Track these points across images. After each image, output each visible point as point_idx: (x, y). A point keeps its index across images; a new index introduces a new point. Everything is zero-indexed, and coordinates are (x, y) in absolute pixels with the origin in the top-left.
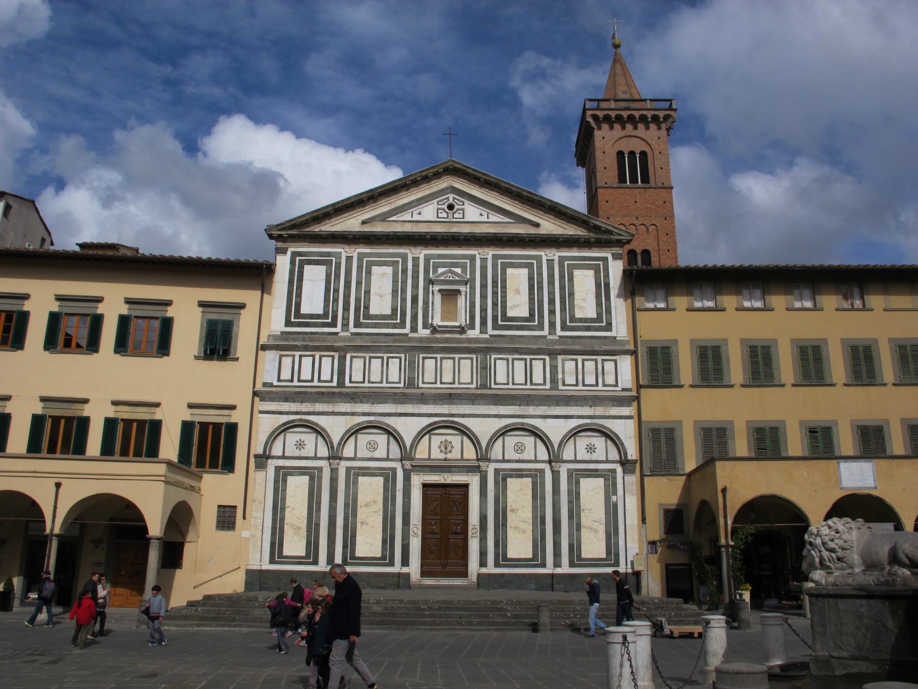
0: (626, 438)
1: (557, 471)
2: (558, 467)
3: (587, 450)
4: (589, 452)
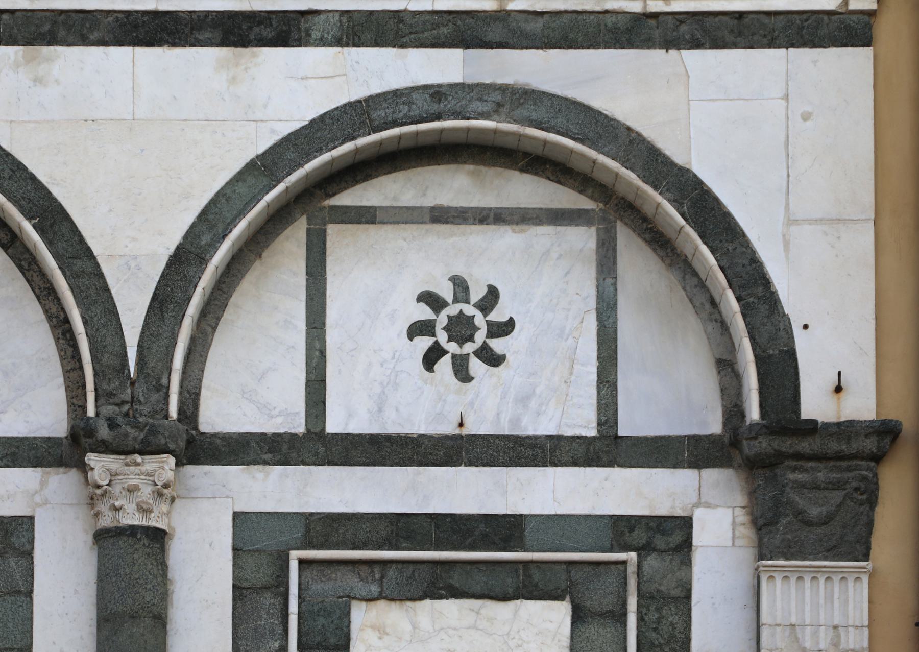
0: (791, 221)
1: (132, 531)
2: (146, 491)
3: (424, 343)
4: (444, 365)
